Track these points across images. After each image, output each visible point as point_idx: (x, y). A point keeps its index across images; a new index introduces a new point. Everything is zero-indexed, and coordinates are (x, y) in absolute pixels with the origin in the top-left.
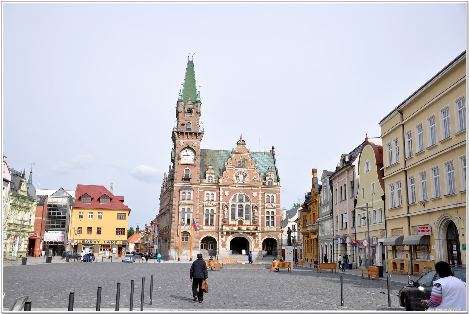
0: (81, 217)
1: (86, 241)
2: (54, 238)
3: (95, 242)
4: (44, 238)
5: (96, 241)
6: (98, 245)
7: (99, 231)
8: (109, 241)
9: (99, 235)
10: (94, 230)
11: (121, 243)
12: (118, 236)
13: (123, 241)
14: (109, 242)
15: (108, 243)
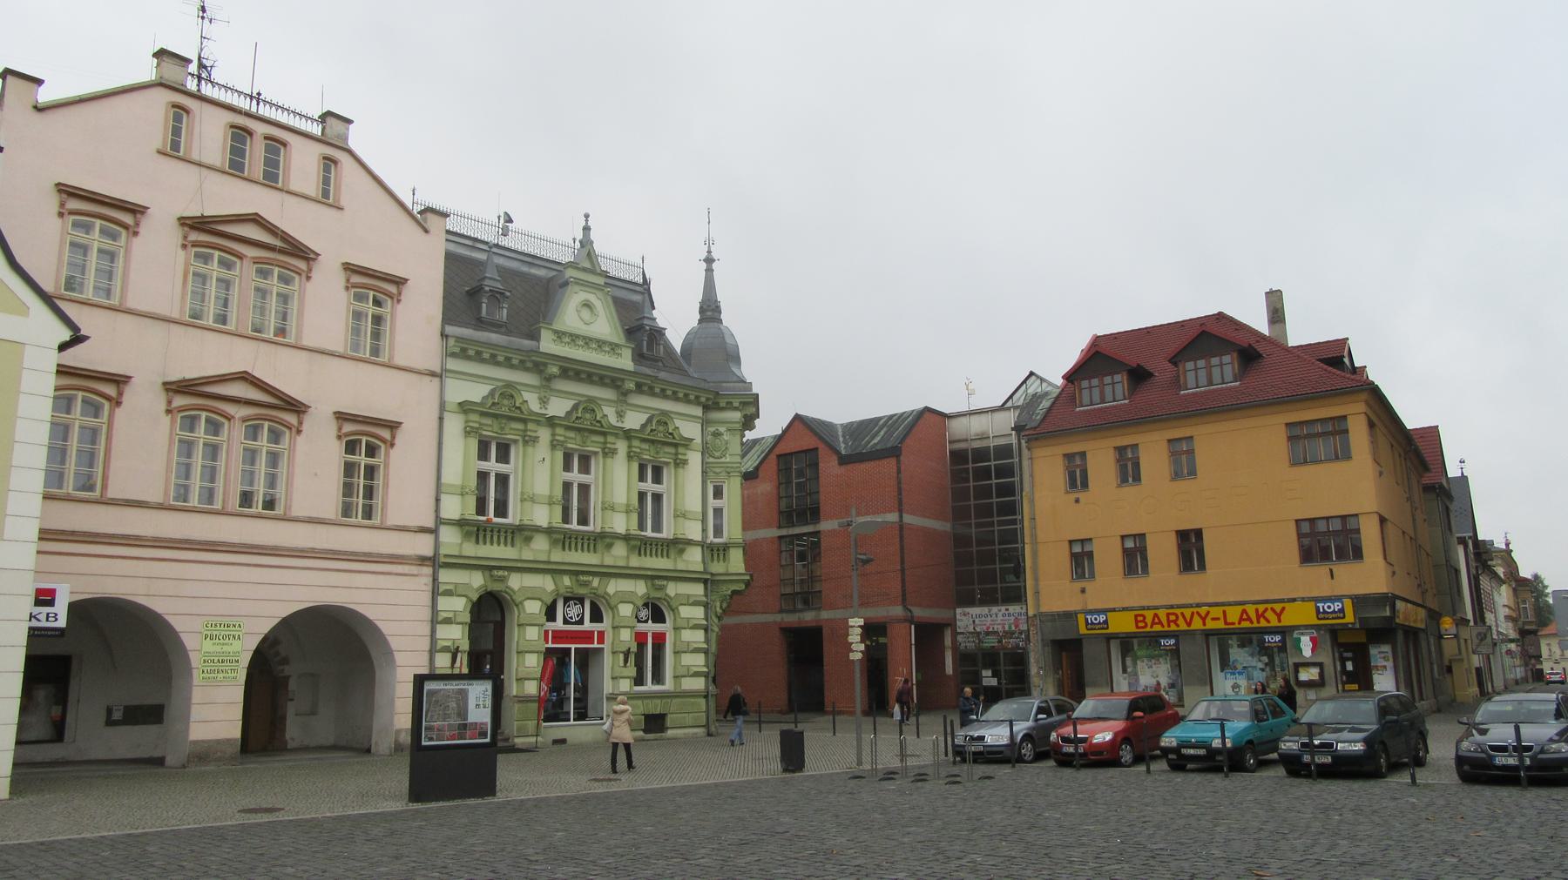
0: (1077, 479)
1: (1149, 615)
2: (1000, 615)
3: (1188, 617)
4: (958, 617)
5: (1193, 614)
6: (1200, 639)
7: (1190, 547)
8: (1244, 611)
9: (1192, 578)
10: (1163, 552)
11: (1349, 618)
12: (1319, 571)
13: (1360, 601)
14: (1244, 616)
15: (1246, 624)
